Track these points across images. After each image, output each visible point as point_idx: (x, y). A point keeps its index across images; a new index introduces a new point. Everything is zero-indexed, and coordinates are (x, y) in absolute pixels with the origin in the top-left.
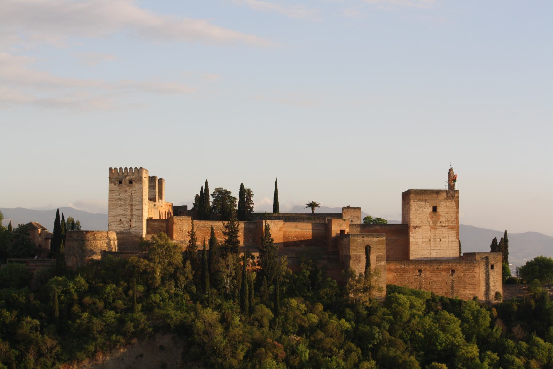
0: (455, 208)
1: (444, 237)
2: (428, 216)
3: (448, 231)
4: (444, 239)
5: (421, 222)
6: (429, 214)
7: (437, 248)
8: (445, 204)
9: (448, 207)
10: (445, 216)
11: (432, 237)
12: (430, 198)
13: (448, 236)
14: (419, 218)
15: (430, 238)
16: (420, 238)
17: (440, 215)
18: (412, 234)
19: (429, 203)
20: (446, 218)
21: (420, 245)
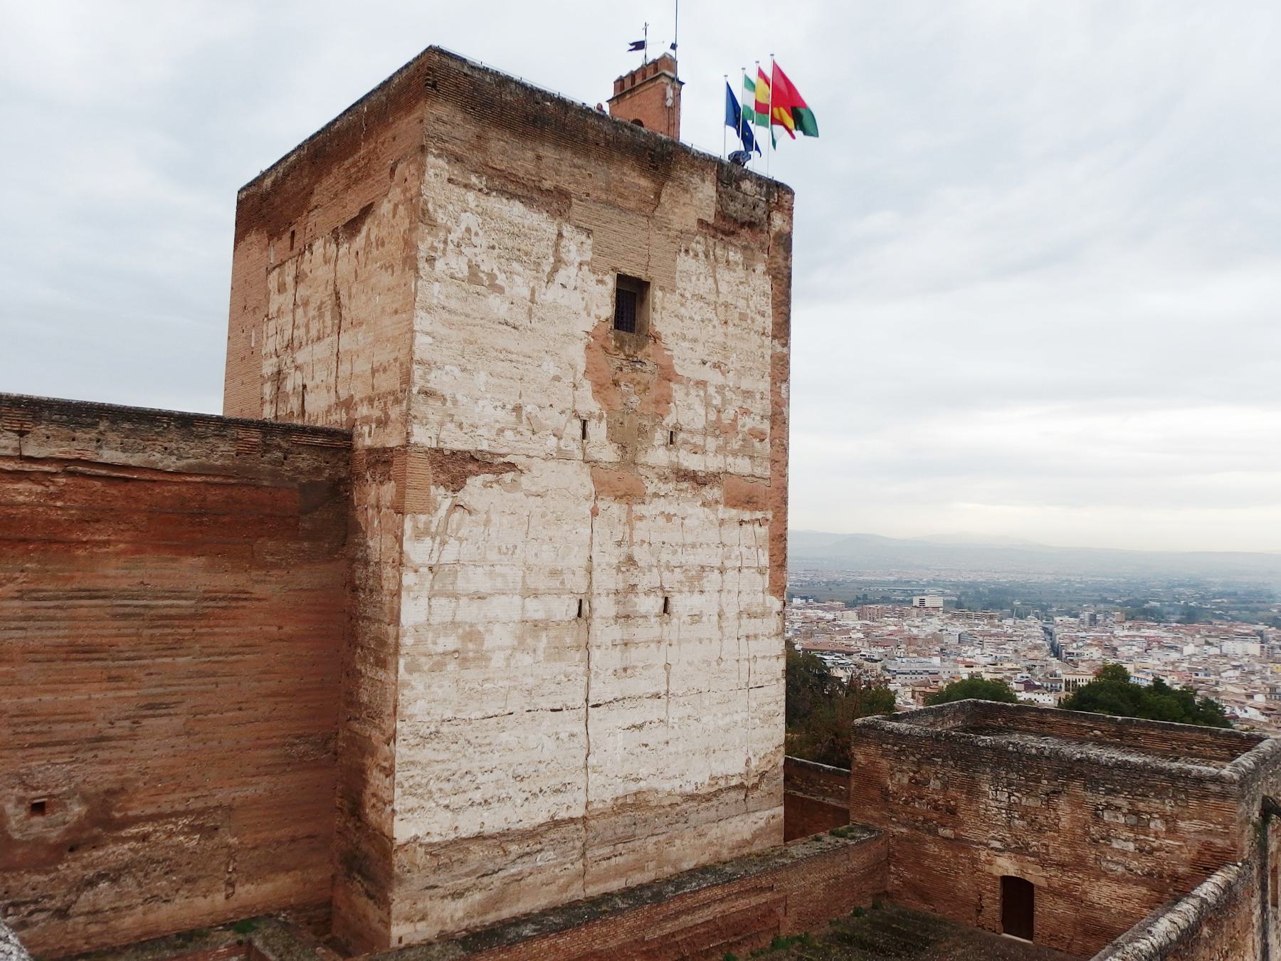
0: (769, 324)
1: (696, 578)
2: (582, 367)
3: (722, 522)
4: (691, 592)
5: (512, 418)
6: (588, 347)
7: (643, 686)
8: (711, 280)
9: (726, 305)
10: (702, 384)
11: (606, 580)
12: (604, 197)
13: (722, 571)
14: (500, 367)
15: (580, 584)
16: (499, 584)
17: (667, 375)
18: (428, 540)
19: (589, 232)
20: (708, 405)
21: (498, 660)
